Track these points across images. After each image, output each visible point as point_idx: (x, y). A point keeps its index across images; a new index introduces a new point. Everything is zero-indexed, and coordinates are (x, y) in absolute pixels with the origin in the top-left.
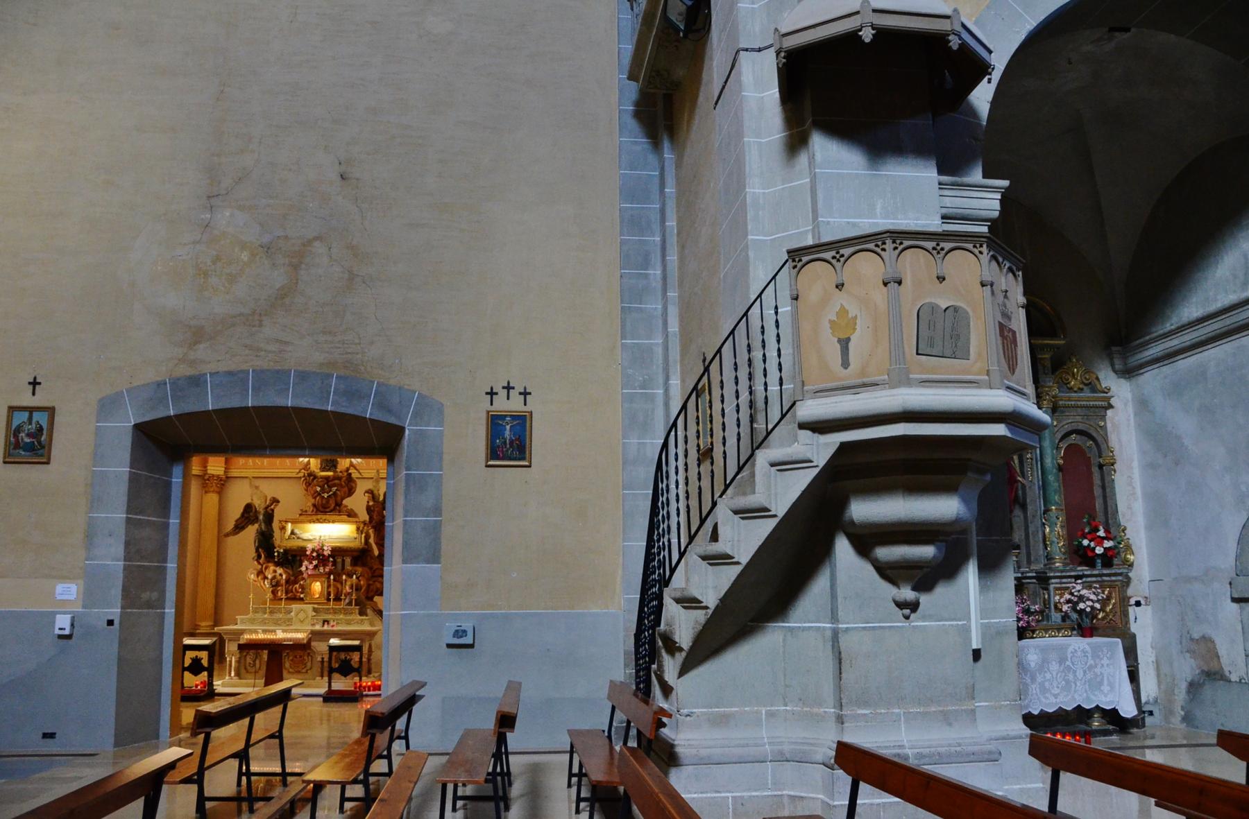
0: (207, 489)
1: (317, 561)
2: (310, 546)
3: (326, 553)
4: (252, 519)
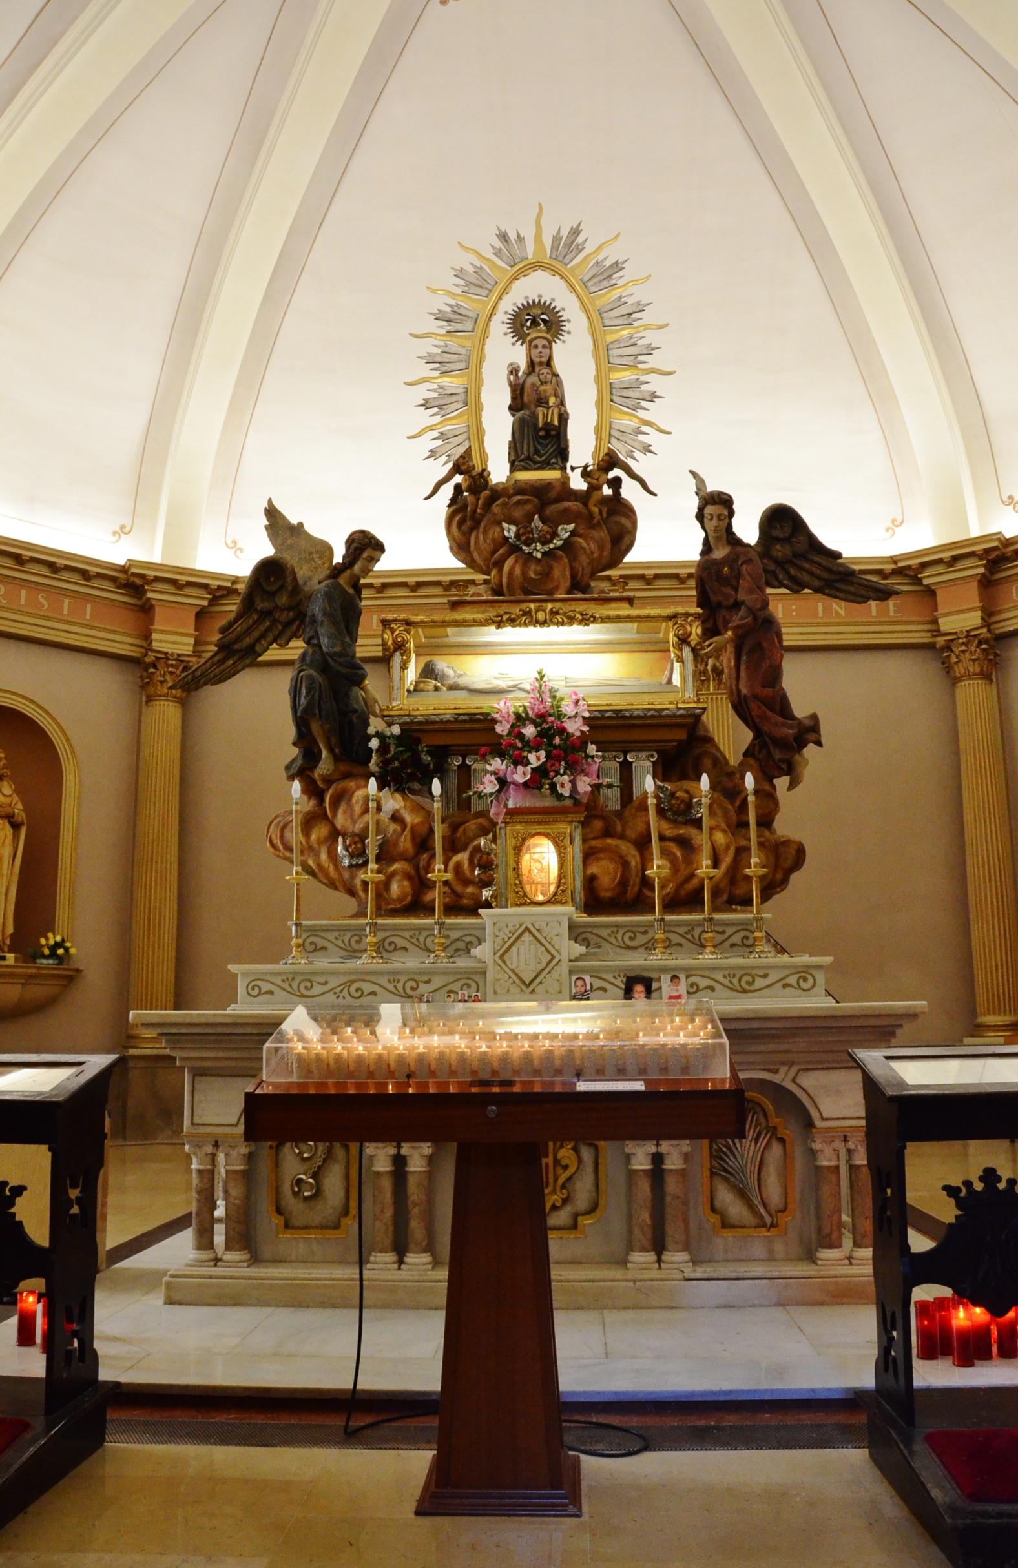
0: (151, 690)
1: (542, 754)
2: (504, 708)
3: (575, 727)
4: (284, 617)
